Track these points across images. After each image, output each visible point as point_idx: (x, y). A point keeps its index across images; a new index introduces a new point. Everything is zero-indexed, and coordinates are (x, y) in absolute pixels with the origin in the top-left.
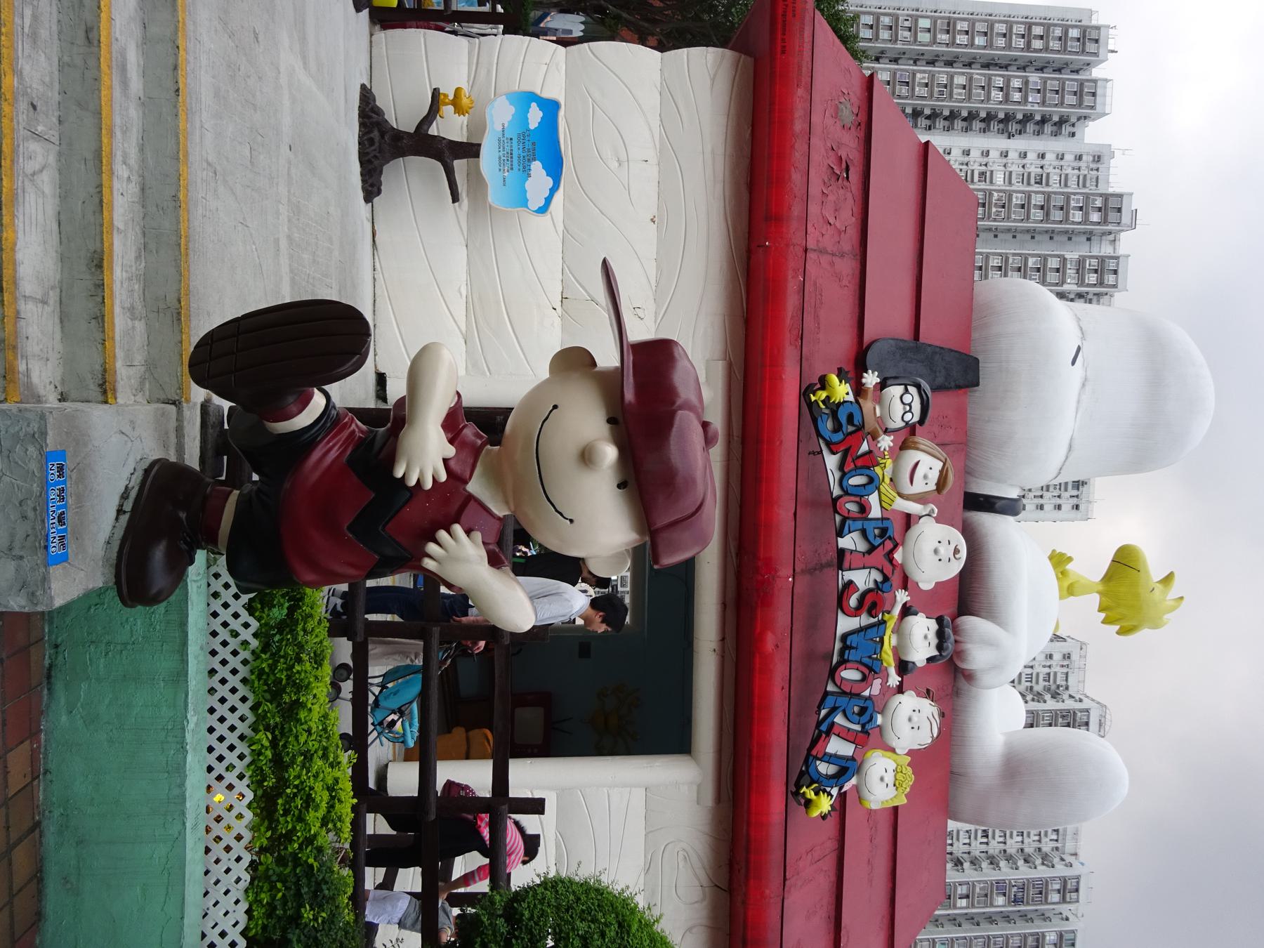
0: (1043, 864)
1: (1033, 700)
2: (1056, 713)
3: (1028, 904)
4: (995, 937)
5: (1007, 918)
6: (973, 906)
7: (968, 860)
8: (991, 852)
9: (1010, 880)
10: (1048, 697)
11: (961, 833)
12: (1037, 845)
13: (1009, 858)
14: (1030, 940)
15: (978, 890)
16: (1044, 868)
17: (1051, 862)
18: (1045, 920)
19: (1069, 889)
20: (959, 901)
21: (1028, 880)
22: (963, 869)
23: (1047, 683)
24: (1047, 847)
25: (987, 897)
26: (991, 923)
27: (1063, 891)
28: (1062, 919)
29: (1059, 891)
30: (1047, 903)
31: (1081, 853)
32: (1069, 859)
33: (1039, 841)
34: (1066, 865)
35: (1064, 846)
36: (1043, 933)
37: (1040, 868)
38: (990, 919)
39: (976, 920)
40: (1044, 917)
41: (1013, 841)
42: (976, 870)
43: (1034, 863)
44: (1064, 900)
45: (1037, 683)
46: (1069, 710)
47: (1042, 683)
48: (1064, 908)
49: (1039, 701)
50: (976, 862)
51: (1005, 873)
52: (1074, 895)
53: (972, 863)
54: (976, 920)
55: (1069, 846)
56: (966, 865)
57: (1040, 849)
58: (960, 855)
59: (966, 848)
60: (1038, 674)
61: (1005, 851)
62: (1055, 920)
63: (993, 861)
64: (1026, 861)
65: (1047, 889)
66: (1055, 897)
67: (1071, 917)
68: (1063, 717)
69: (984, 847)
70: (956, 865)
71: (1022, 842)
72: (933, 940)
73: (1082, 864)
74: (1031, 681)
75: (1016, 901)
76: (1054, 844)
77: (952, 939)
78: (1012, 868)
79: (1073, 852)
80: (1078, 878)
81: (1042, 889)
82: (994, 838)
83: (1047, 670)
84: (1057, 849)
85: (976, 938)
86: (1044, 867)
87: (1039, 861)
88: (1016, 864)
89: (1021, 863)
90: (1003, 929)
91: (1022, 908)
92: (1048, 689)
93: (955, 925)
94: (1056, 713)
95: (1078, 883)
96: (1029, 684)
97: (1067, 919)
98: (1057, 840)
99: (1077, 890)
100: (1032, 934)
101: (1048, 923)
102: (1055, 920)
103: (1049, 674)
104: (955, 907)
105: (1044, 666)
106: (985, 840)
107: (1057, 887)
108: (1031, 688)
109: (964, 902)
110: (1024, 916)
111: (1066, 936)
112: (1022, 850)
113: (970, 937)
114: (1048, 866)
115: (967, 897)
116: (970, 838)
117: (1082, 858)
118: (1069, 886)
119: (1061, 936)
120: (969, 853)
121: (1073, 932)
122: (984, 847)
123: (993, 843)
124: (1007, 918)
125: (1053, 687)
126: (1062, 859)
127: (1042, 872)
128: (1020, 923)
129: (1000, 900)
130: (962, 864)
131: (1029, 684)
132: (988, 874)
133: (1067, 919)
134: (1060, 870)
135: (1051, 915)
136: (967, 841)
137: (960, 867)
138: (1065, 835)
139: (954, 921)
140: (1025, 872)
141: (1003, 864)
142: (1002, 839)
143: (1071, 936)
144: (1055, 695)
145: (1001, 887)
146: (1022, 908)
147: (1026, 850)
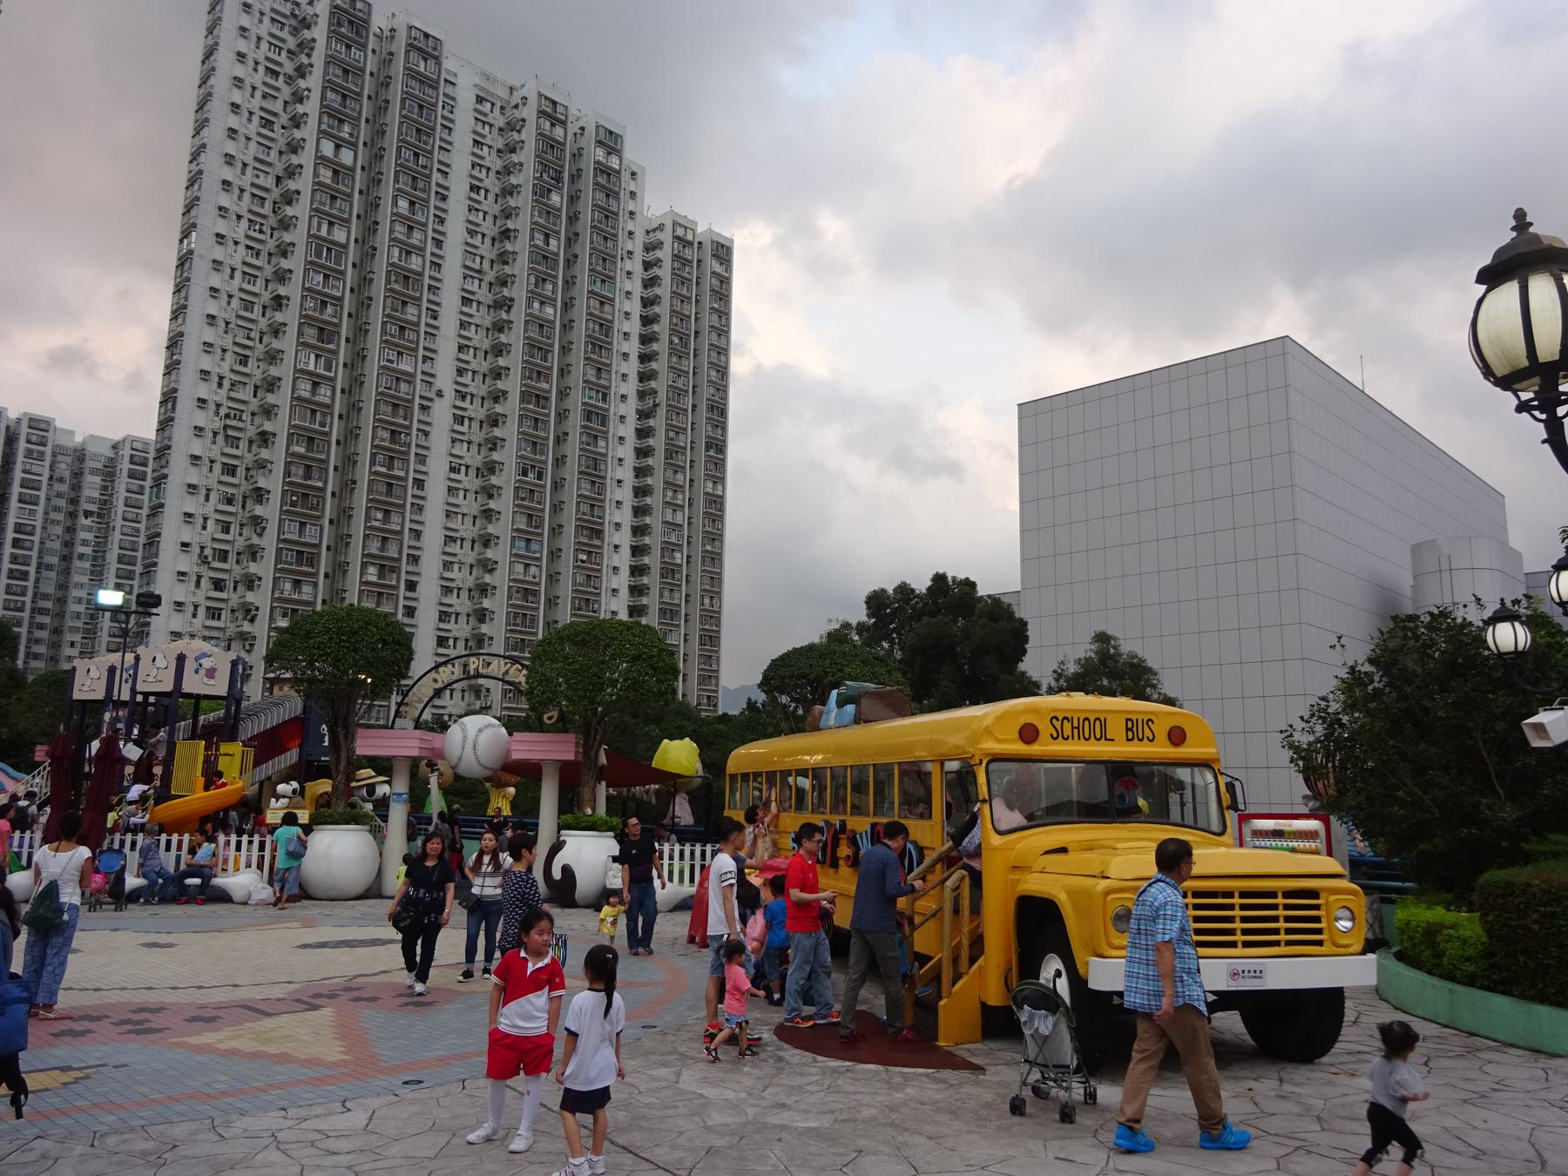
0: (519, 132)
1: (309, 56)
2: (333, 31)
3: (562, 166)
4: (593, 220)
5: (573, 199)
6: (558, 232)
7: (504, 222)
8: (497, 190)
9: (535, 178)
10: (307, 34)
11: (471, 218)
12: (495, 131)
13: (507, 170)
14: (599, 179)
15: (541, 221)
16: (524, 131)
17: (518, 121)
18: (581, 155)
19: (552, 112)
20: (551, 248)
21: (536, 156)
22: (515, 230)
23: (286, 28)
24: (500, 121)
25: (550, 212)
26: (577, 219)
27: (555, 121)
28: (582, 134)
29: (553, 125)
30: (564, 144)
31: (511, 82)
32: (516, 99)
33: (491, 126)
34: (524, 104)
35: (501, 99)
36: (596, 162)
37: (523, 136)
38: (573, 219)
39: (572, 236)
40: (577, 155)
41: (488, 159)
42: (517, 215)
43: (517, 142)
44: (563, 123)
45: (283, 41)
46: (331, 13)
47: (285, 34)
48: (573, 128)
49: (312, 49)
50: (507, 212)
51: (525, 178)
52: (559, 109)
53: (508, 217)
54: (572, 236)
55: (504, 94)
56: (510, 225)
57: (501, 129)
58: (497, 230)
59: (489, 219)
60: (271, 35)
61: (498, 172)
62: (583, 143)
63: (509, 191)
64: (513, 151)
65: (549, 138)
66: (558, 132)
67: (581, 124)
68: (339, 24)
69: (491, 197)
70: (508, 238)
71: (490, 147)
72: (589, 292)
73: (523, 86)
74: (281, 49)
75: (558, 179)
76: (497, 109)
77: (590, 270)
78: (520, 170)
79: (508, 91)
80: (540, 95)
81: (549, 144)
82: (481, 180)
83: (266, 20)
84: (502, 108)
85: (592, 242)
86: (524, 131)
87: (516, 136)
88: (515, 164)
89: (515, 158)
90: (586, 207)
91: (566, 175)
92: (295, 31)
93: (575, 262)
94: (333, 31)
95: (546, 98)
96: (284, 53)
97: (582, 129)
98: (493, 104)
99: (554, 103)
100: (595, 176)
101: (585, 152)
102: (583, 143)
103: (273, 20)
104: (557, 255)
105: (261, 21)
106: (482, 192)
107: (547, 125)
108: (289, 51)
109: (553, 242)
110: (574, 178)
111: (602, 137)
112: (499, 151)
113: (591, 248)
114: (522, 127)
115: (547, 236)
116: (477, 210)
117: (517, 84)
118: (549, 110)
119: (600, 143)
120: (495, 217)
121: (597, 127)
122: (491, 197)
123: (487, 183)
124: (573, 199)
125: (293, 22)
126: (516, 107)
127: (529, 135)
128: (581, 185)
129: (555, 198)
130: (508, 230)
131: (284, 53)
132: (524, 201)
133: (582, 129)
134: (529, 113)
135: (576, 146)
136: (481, 214)
137: (512, 234)
138: (488, 92)
139: (571, 261)
140: (527, 156)
141: (514, 180)
142: (484, 171)
143: (602, 131)
144: (306, 24)
145: (542, 192)
146: (566, 175)
147: (500, 146)
